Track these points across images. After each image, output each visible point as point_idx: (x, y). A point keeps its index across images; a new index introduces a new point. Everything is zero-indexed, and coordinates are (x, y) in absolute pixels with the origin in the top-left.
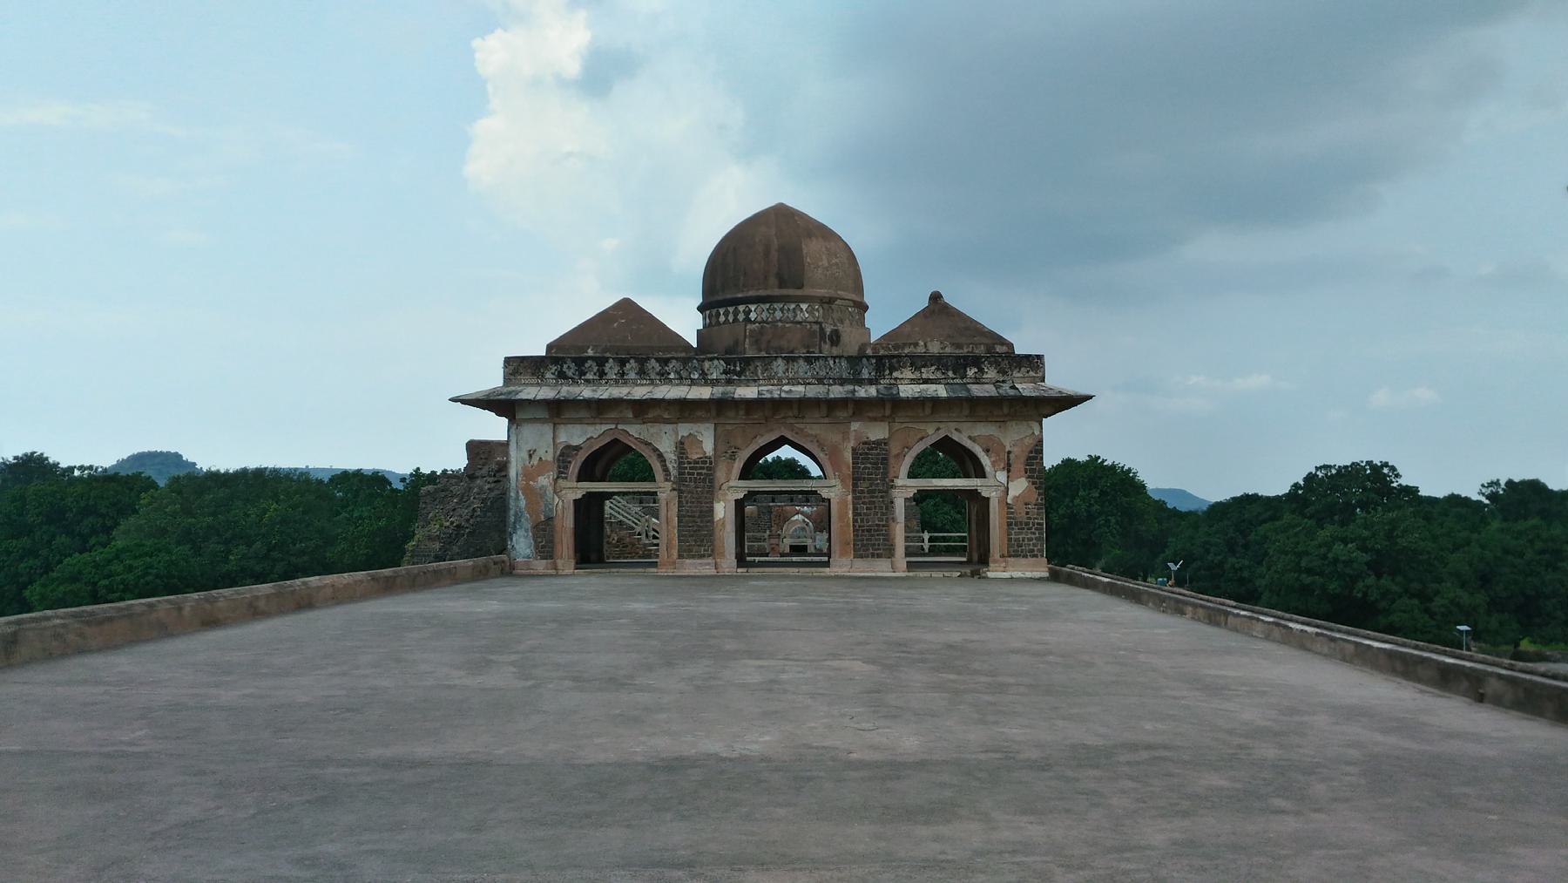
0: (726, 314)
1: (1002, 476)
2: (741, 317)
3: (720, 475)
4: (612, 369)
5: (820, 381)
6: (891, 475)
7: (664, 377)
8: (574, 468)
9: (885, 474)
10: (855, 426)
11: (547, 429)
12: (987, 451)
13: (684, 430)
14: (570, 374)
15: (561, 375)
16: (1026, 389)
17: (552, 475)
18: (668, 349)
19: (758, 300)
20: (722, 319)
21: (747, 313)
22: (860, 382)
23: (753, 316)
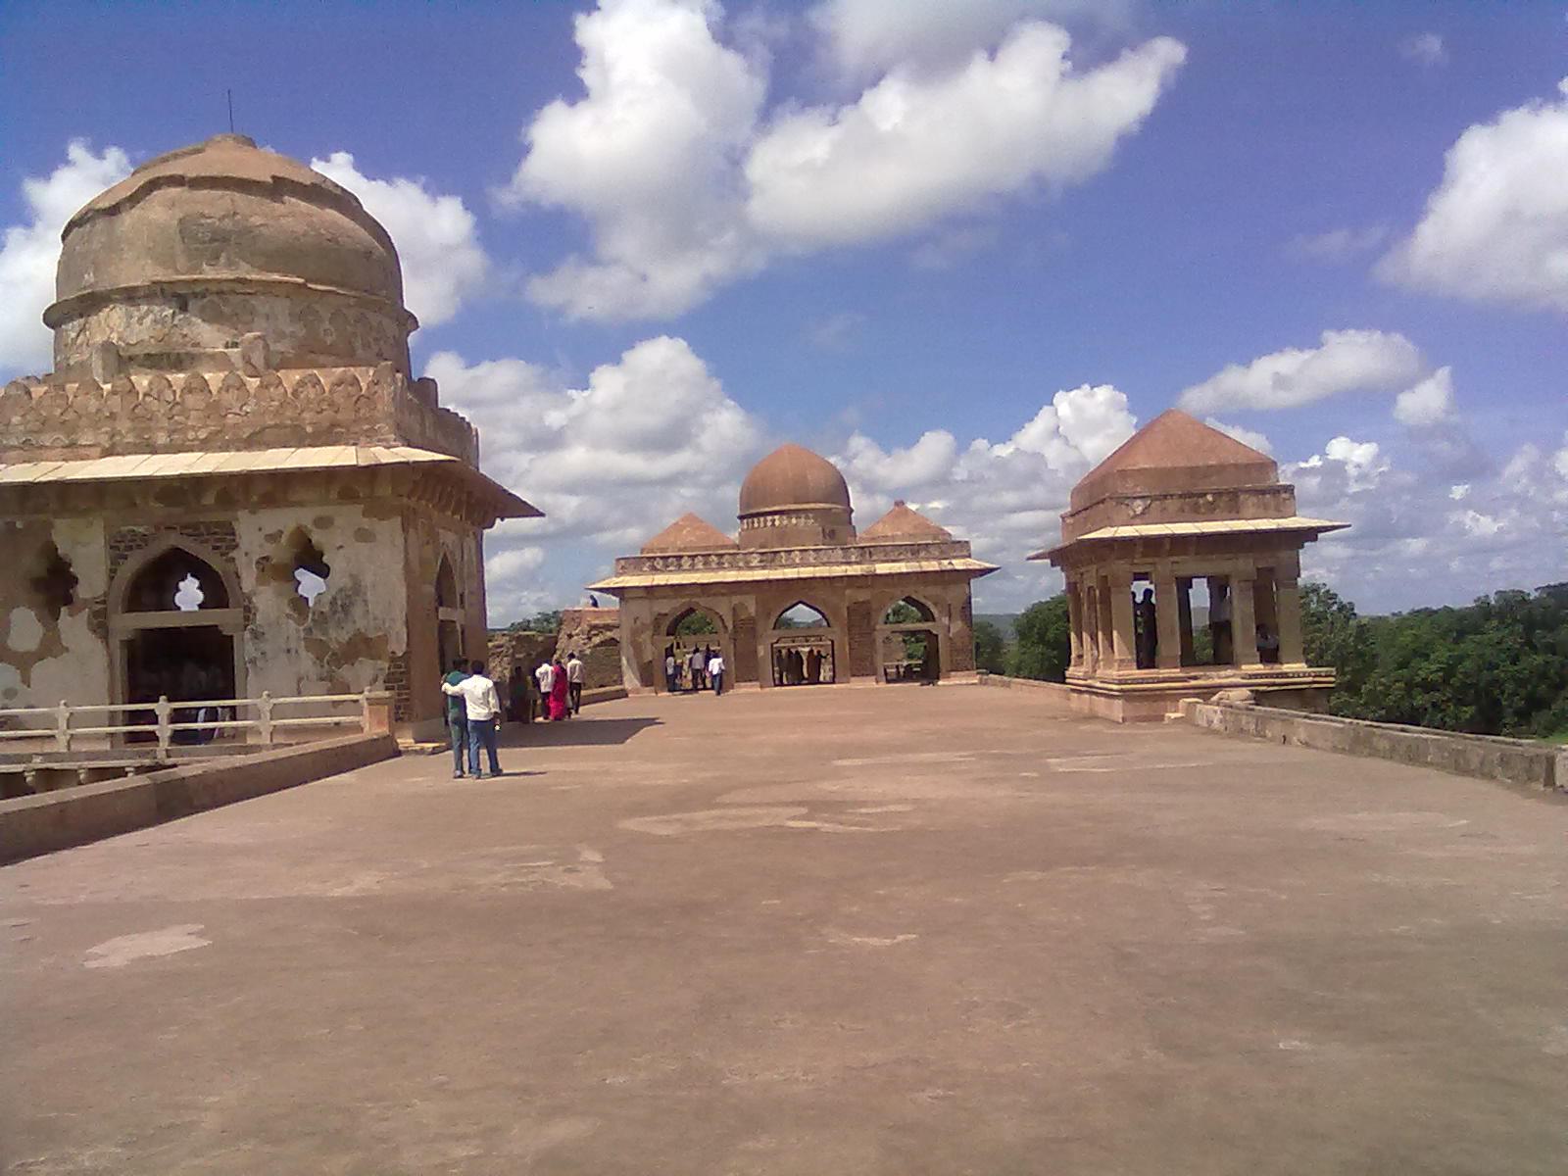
0: (759, 523)
1: (945, 620)
2: (769, 524)
3: (760, 628)
4: (686, 563)
5: (824, 564)
6: (872, 623)
7: (720, 566)
8: (664, 628)
9: (869, 623)
10: (848, 592)
11: (646, 602)
12: (936, 604)
13: (736, 600)
14: (659, 567)
15: (654, 569)
16: (959, 564)
17: (649, 633)
18: (723, 547)
19: (780, 513)
20: (756, 525)
21: (773, 521)
22: (849, 563)
23: (777, 523)
